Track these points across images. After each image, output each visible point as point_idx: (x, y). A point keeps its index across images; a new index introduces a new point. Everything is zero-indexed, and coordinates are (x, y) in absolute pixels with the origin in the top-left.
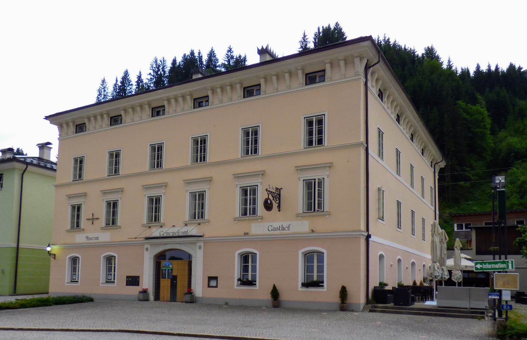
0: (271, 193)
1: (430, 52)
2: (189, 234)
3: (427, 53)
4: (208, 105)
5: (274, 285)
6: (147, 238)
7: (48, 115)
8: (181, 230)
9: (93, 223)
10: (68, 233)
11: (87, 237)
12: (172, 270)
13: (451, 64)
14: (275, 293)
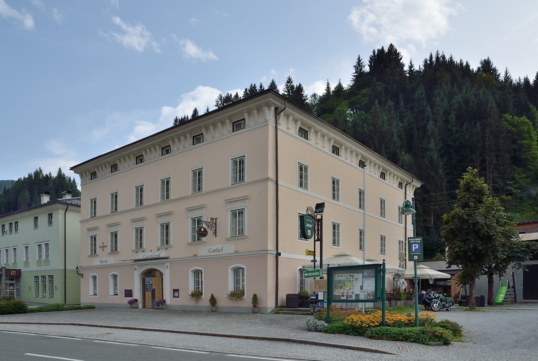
0: (205, 223)
1: (486, 65)
2: (161, 256)
3: (483, 67)
4: (171, 153)
5: (212, 295)
6: (136, 261)
7: (72, 167)
8: (156, 254)
9: (103, 250)
10: (89, 258)
11: (100, 261)
12: (152, 285)
13: (508, 75)
14: (213, 301)
